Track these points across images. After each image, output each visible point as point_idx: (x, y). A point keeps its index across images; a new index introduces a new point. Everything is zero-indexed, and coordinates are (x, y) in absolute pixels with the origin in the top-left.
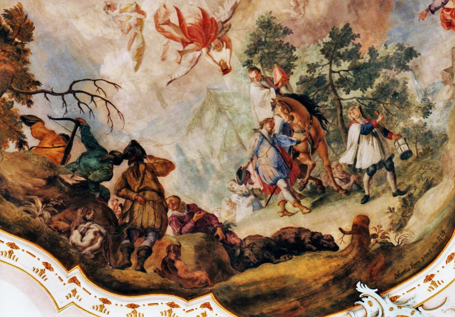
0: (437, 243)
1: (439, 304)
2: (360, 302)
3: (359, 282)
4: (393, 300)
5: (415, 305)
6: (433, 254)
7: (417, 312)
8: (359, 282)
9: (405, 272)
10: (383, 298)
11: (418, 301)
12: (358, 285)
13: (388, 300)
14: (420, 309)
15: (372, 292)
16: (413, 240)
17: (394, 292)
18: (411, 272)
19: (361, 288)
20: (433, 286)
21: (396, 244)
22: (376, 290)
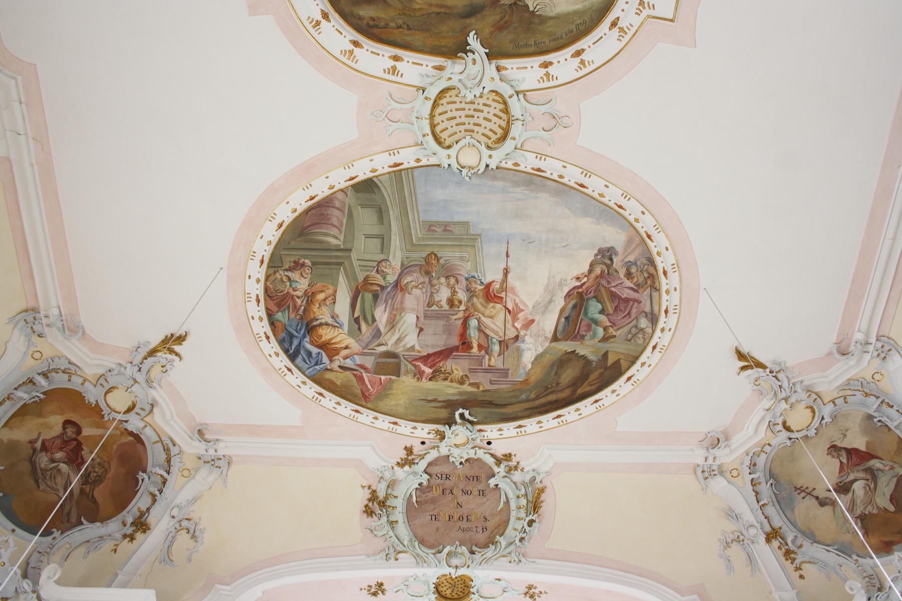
0: (572, 31)
1: (542, 102)
2: (464, 55)
3: (474, 32)
4: (498, 69)
5: (518, 89)
6: (562, 42)
7: (515, 96)
8: (474, 32)
9: (526, 45)
10: (490, 63)
11: (523, 87)
12: (472, 34)
13: (493, 66)
14: (521, 96)
15: (483, 51)
16: (552, 14)
17: (504, 62)
18: (532, 49)
19: (473, 41)
20: (545, 78)
21: (531, 9)
22: (487, 51)
